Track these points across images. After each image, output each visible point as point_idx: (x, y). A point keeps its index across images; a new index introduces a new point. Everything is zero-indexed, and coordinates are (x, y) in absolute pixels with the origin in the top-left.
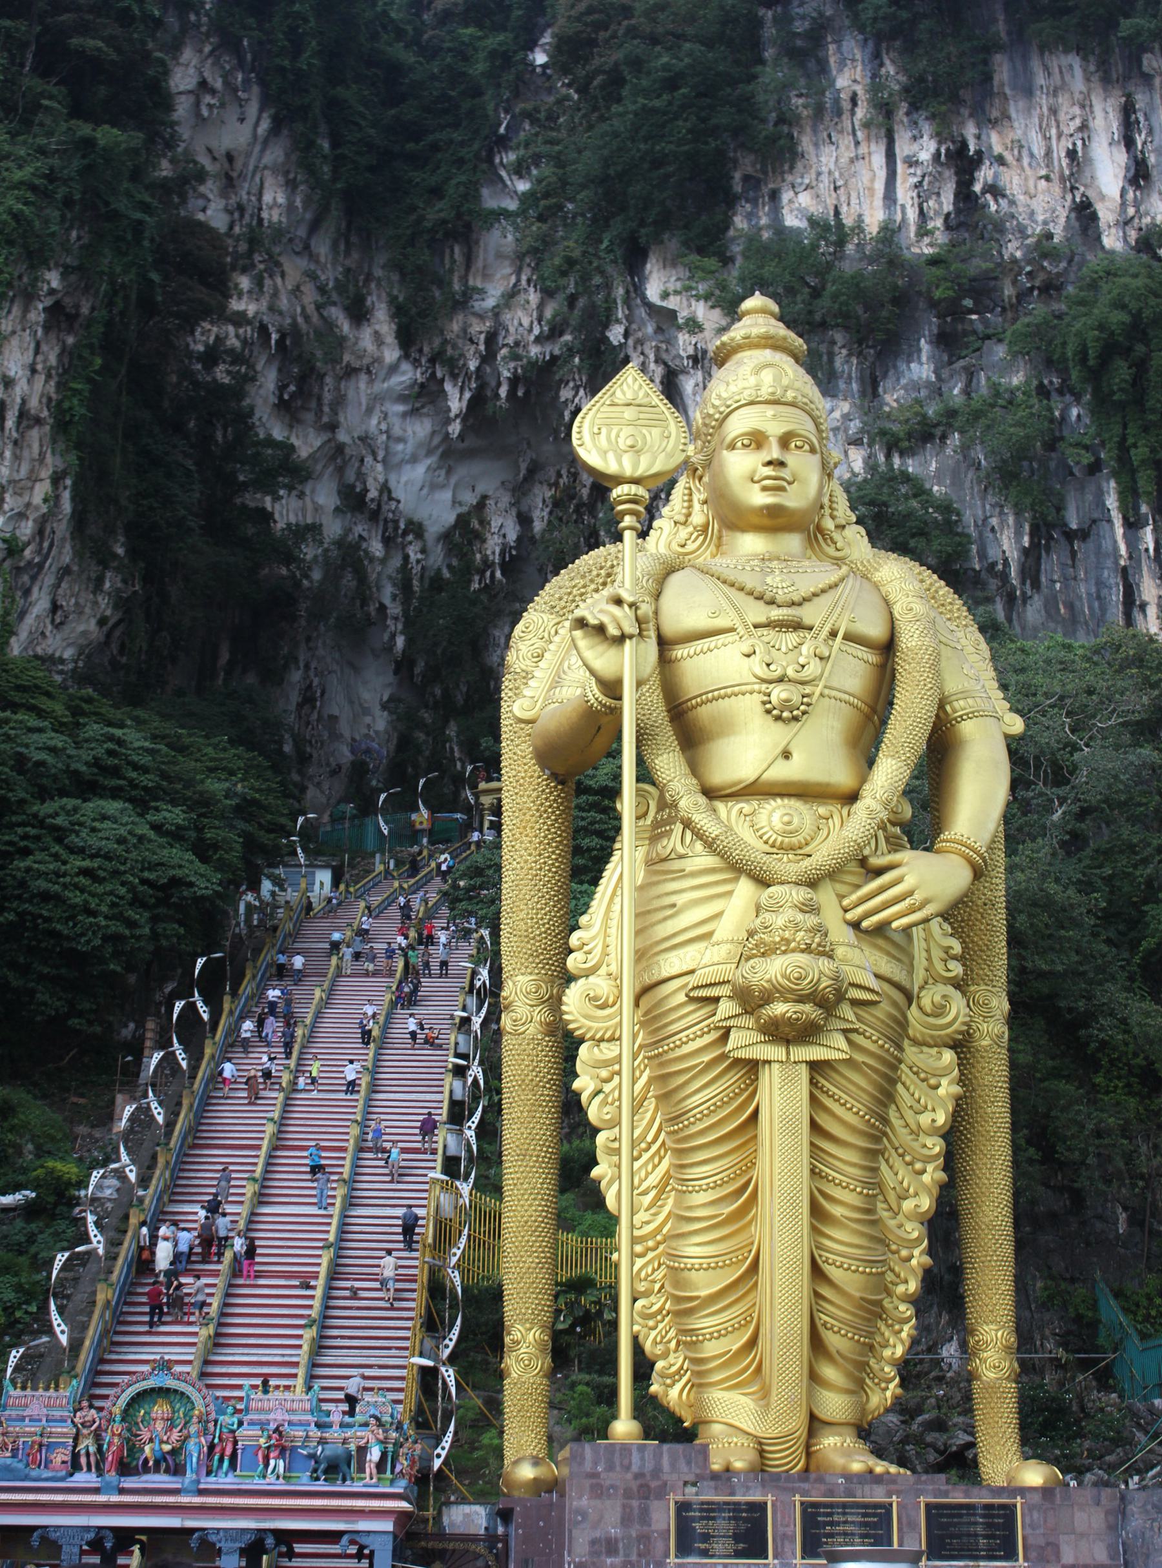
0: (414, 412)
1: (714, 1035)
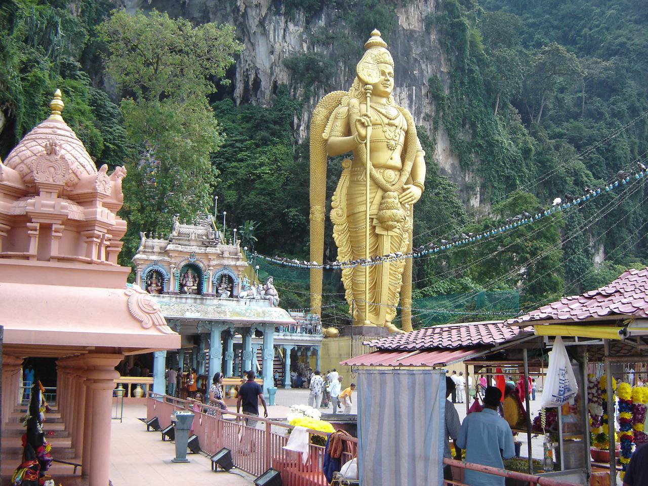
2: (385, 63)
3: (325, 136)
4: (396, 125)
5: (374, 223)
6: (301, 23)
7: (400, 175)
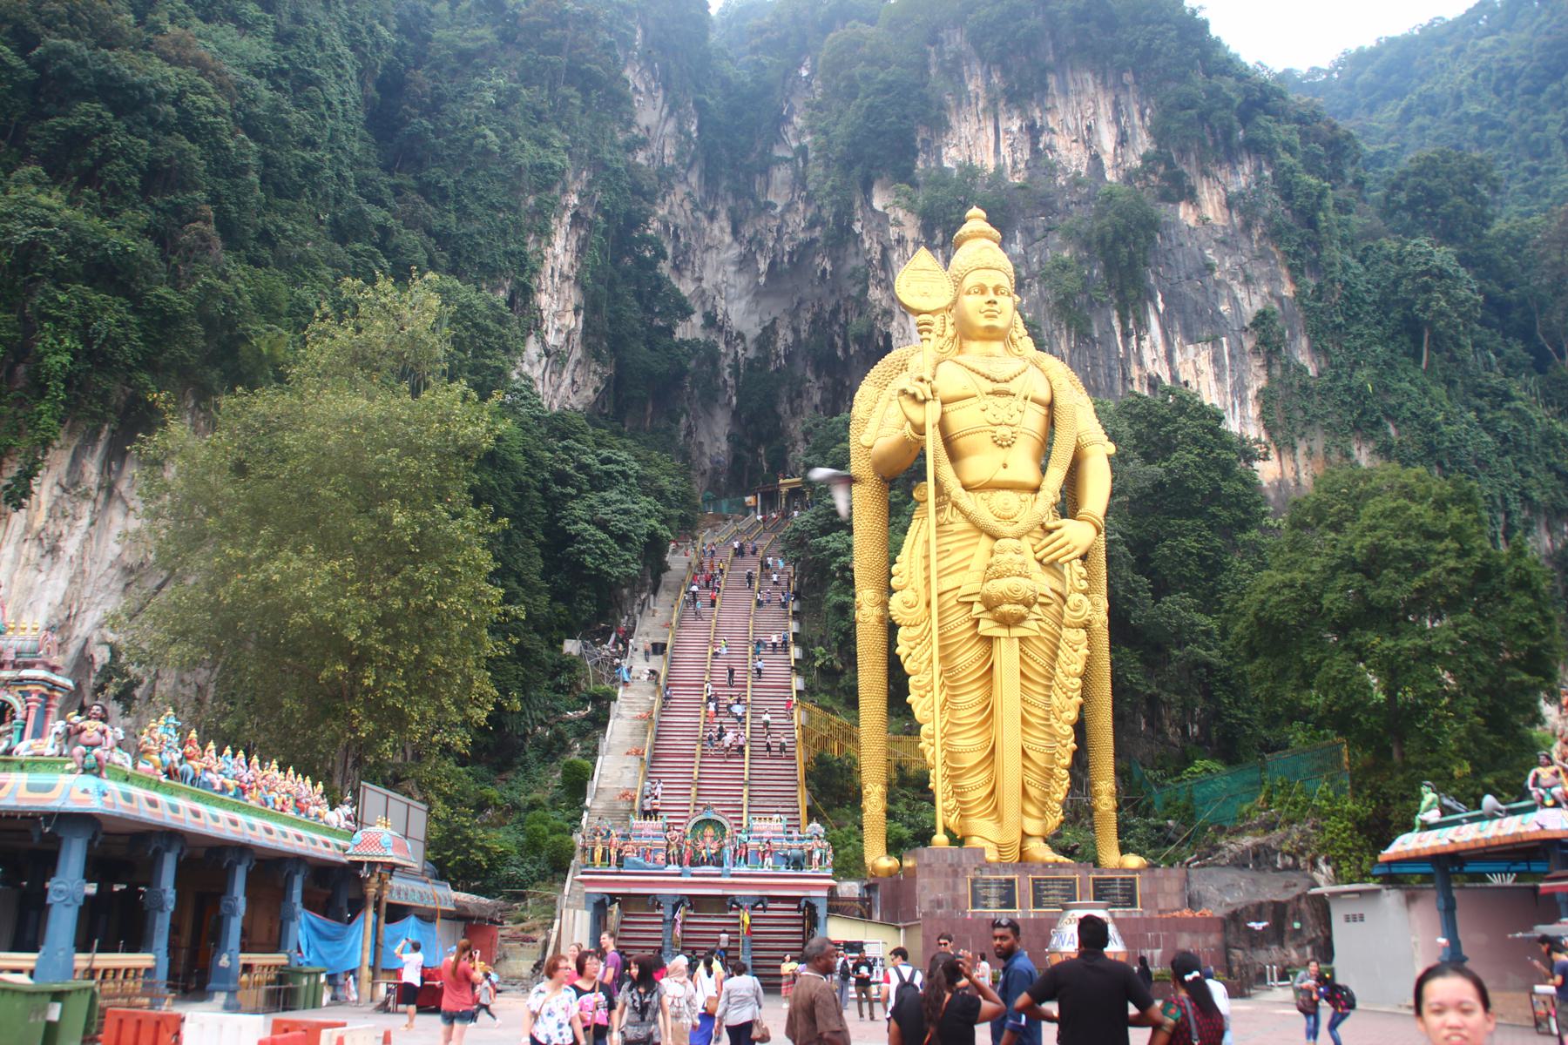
0: (740, 271)
3: (865, 439)
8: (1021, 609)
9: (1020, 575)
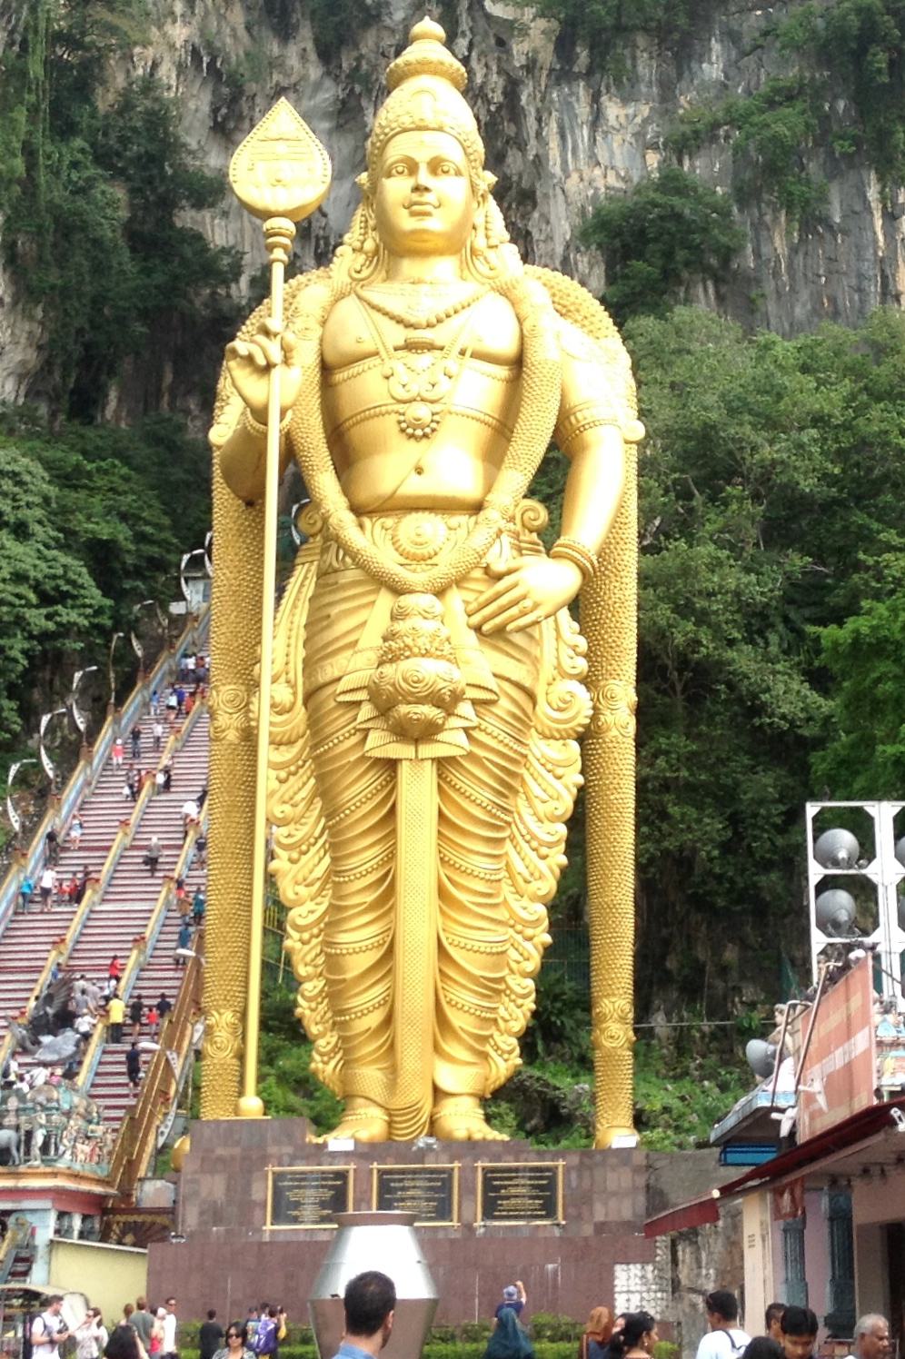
0: (339, 128)
1: (358, 737)
2: (419, 128)
4: (438, 343)
5: (360, 719)
6: (644, 89)
7: (476, 523)
8: (429, 711)
9: (426, 654)
